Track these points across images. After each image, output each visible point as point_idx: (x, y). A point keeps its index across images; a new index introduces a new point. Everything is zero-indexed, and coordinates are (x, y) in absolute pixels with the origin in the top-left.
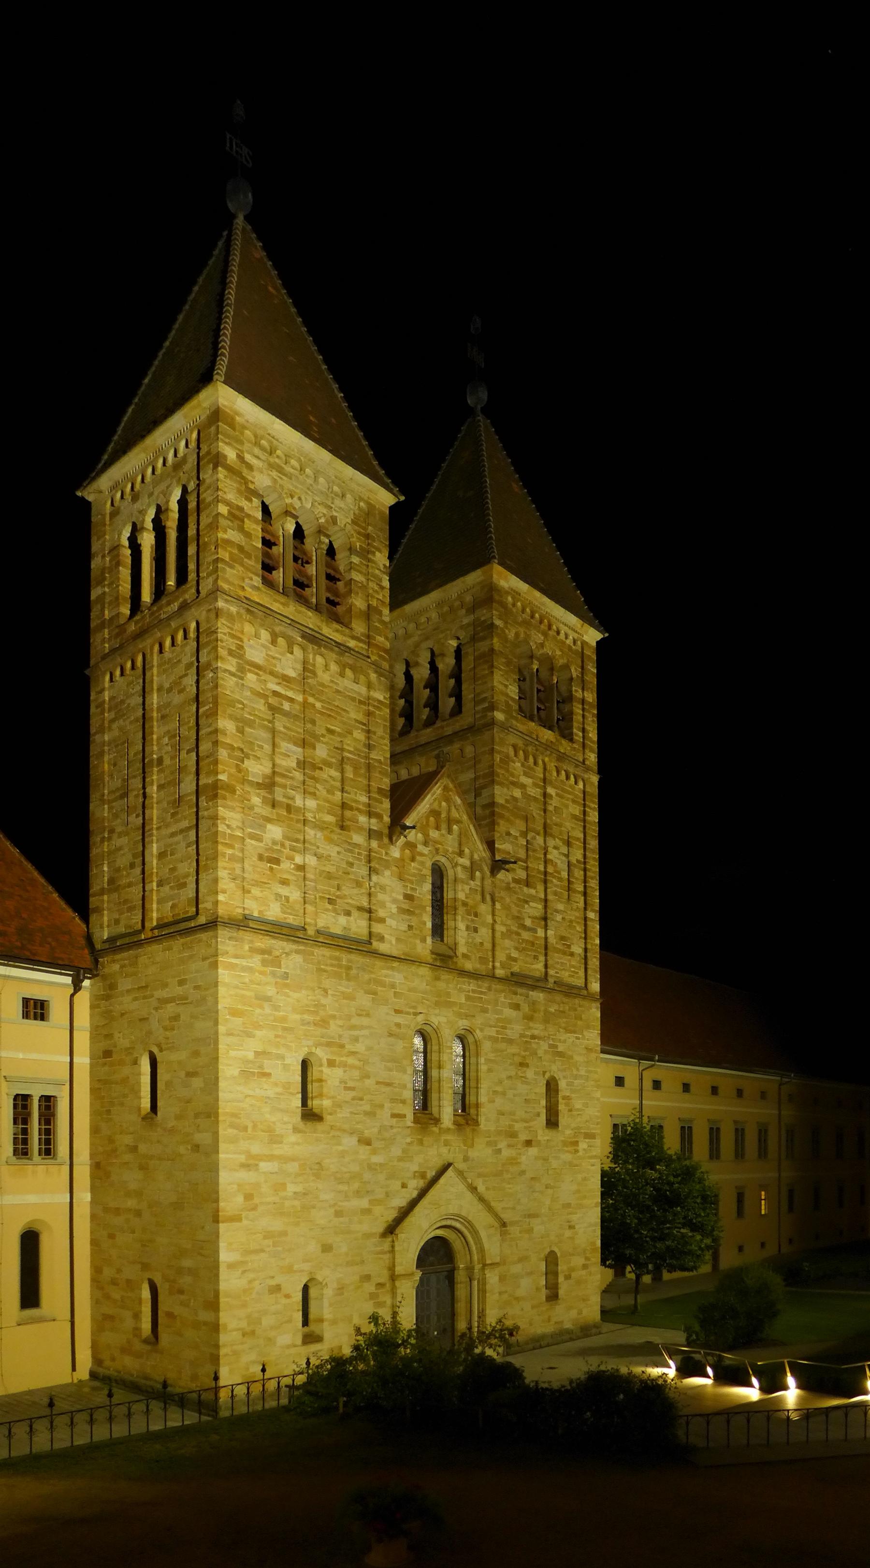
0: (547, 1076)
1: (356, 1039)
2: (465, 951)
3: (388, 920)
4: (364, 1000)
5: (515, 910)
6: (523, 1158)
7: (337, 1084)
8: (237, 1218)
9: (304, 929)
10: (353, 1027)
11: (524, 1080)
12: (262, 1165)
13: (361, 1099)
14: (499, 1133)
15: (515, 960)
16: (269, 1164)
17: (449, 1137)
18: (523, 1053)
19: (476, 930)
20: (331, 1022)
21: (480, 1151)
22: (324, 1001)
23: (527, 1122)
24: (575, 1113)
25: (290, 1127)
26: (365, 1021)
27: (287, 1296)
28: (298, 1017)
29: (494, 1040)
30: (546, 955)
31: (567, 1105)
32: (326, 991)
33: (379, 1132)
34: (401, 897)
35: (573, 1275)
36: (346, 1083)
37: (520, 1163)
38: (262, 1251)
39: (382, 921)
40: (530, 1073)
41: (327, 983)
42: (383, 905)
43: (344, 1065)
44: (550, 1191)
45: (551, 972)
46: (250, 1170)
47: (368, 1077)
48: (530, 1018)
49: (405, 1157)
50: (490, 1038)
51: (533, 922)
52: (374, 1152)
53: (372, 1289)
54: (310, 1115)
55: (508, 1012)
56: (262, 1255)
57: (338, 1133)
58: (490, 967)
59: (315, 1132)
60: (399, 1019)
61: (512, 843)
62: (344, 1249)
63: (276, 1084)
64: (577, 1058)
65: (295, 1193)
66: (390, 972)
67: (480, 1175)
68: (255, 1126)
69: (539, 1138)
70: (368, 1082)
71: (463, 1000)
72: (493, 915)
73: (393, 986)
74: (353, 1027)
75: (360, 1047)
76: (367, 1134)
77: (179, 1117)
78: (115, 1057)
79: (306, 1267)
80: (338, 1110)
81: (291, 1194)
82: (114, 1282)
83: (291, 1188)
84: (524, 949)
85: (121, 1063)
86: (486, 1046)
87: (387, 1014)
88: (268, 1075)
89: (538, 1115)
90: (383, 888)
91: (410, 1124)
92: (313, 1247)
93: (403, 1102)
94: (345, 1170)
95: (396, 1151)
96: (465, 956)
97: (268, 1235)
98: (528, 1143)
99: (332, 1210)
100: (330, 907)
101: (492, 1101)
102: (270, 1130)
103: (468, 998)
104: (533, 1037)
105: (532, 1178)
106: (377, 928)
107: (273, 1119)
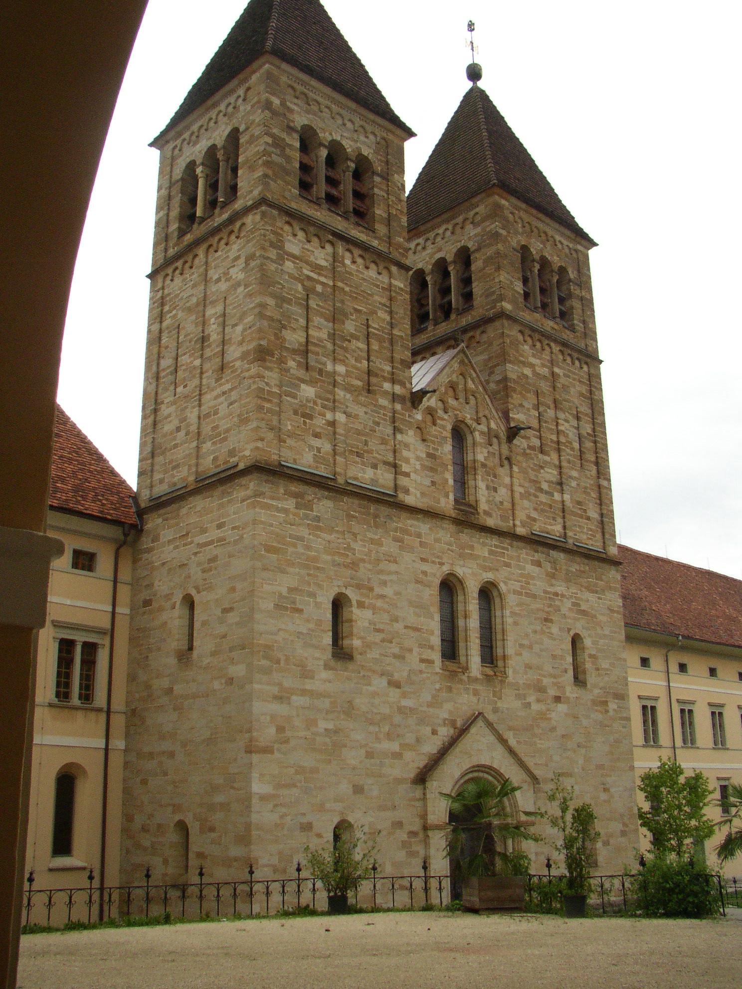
0: (572, 633)
1: (384, 583)
2: (486, 508)
3: (413, 476)
4: (390, 546)
5: (532, 475)
6: (553, 715)
7: (366, 624)
8: (267, 750)
9: (334, 480)
10: (381, 572)
11: (551, 636)
12: (294, 698)
13: (391, 642)
14: (528, 686)
15: (534, 520)
16: (302, 698)
17: (478, 687)
18: (547, 609)
19: (495, 490)
20: (361, 565)
21: (509, 702)
22: (353, 545)
23: (555, 677)
25: (322, 663)
26: (393, 567)
27: (319, 836)
28: (329, 558)
30: (564, 517)
31: (593, 663)
33: (409, 676)
34: (424, 456)
35: (612, 841)
36: (375, 625)
37: (550, 719)
38: (296, 786)
39: (407, 475)
40: (555, 630)
41: (356, 528)
42: (407, 461)
43: (373, 608)
44: (583, 751)
45: (570, 534)
46: (282, 703)
47: (396, 620)
48: (553, 576)
49: (435, 703)
50: (515, 592)
51: (549, 486)
52: (404, 695)
53: (405, 837)
56: (294, 790)
57: (369, 674)
58: (511, 524)
59: (345, 671)
60: (425, 567)
61: (525, 414)
62: (375, 793)
63: (308, 621)
65: (326, 730)
66: (416, 523)
68: (287, 659)
69: (568, 694)
70: (395, 625)
71: (486, 554)
72: (511, 477)
73: (419, 535)
74: (381, 572)
75: (388, 591)
76: (396, 676)
77: (214, 654)
78: (155, 605)
79: (339, 806)
80: (368, 651)
81: (322, 730)
82: (144, 829)
83: (323, 725)
84: (543, 511)
85: (160, 609)
86: (511, 600)
87: (414, 561)
88: (300, 611)
89: (566, 671)
90: (407, 446)
91: (438, 670)
92: (345, 788)
93: (432, 648)
94: (375, 711)
95: (427, 697)
96: (486, 513)
97: (300, 770)
98: (558, 699)
99: (363, 752)
100: (358, 459)
102: (302, 665)
103: (491, 552)
105: (563, 736)
106: (403, 481)
107: (306, 655)
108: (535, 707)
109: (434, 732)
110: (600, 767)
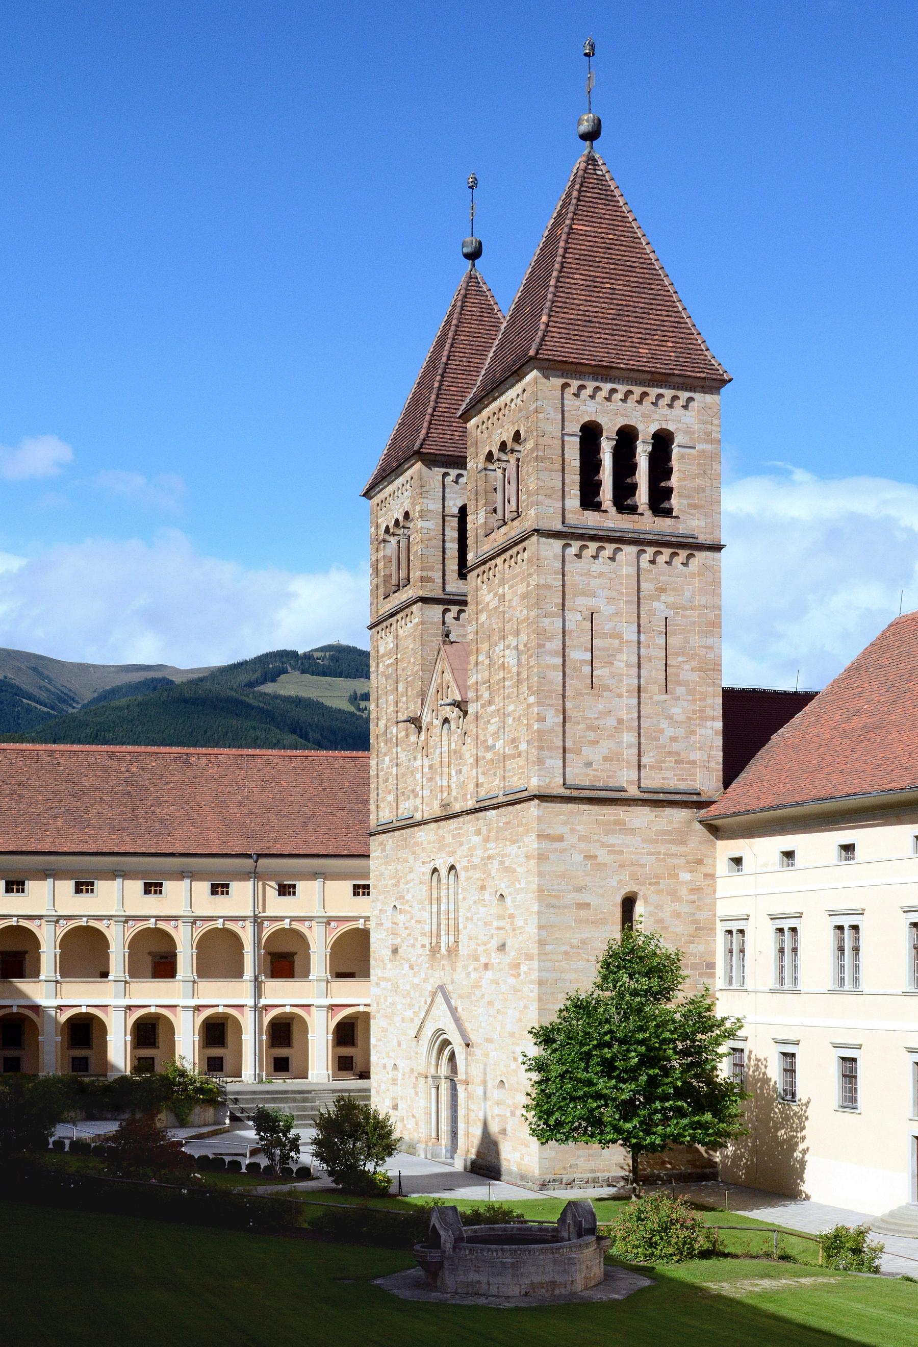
24: (517, 932)
29: (466, 869)
32: (398, 859)
40: (487, 896)
44: (500, 1017)
47: (412, 918)
48: (487, 840)
55: (475, 839)
64: (520, 870)
67: (460, 997)
69: (493, 961)
74: (407, 883)
84: (488, 770)
92: (395, 1043)
95: (423, 975)
101: (465, 928)
103: (454, 837)
104: (489, 858)
108: (474, 976)
110: (512, 1035)
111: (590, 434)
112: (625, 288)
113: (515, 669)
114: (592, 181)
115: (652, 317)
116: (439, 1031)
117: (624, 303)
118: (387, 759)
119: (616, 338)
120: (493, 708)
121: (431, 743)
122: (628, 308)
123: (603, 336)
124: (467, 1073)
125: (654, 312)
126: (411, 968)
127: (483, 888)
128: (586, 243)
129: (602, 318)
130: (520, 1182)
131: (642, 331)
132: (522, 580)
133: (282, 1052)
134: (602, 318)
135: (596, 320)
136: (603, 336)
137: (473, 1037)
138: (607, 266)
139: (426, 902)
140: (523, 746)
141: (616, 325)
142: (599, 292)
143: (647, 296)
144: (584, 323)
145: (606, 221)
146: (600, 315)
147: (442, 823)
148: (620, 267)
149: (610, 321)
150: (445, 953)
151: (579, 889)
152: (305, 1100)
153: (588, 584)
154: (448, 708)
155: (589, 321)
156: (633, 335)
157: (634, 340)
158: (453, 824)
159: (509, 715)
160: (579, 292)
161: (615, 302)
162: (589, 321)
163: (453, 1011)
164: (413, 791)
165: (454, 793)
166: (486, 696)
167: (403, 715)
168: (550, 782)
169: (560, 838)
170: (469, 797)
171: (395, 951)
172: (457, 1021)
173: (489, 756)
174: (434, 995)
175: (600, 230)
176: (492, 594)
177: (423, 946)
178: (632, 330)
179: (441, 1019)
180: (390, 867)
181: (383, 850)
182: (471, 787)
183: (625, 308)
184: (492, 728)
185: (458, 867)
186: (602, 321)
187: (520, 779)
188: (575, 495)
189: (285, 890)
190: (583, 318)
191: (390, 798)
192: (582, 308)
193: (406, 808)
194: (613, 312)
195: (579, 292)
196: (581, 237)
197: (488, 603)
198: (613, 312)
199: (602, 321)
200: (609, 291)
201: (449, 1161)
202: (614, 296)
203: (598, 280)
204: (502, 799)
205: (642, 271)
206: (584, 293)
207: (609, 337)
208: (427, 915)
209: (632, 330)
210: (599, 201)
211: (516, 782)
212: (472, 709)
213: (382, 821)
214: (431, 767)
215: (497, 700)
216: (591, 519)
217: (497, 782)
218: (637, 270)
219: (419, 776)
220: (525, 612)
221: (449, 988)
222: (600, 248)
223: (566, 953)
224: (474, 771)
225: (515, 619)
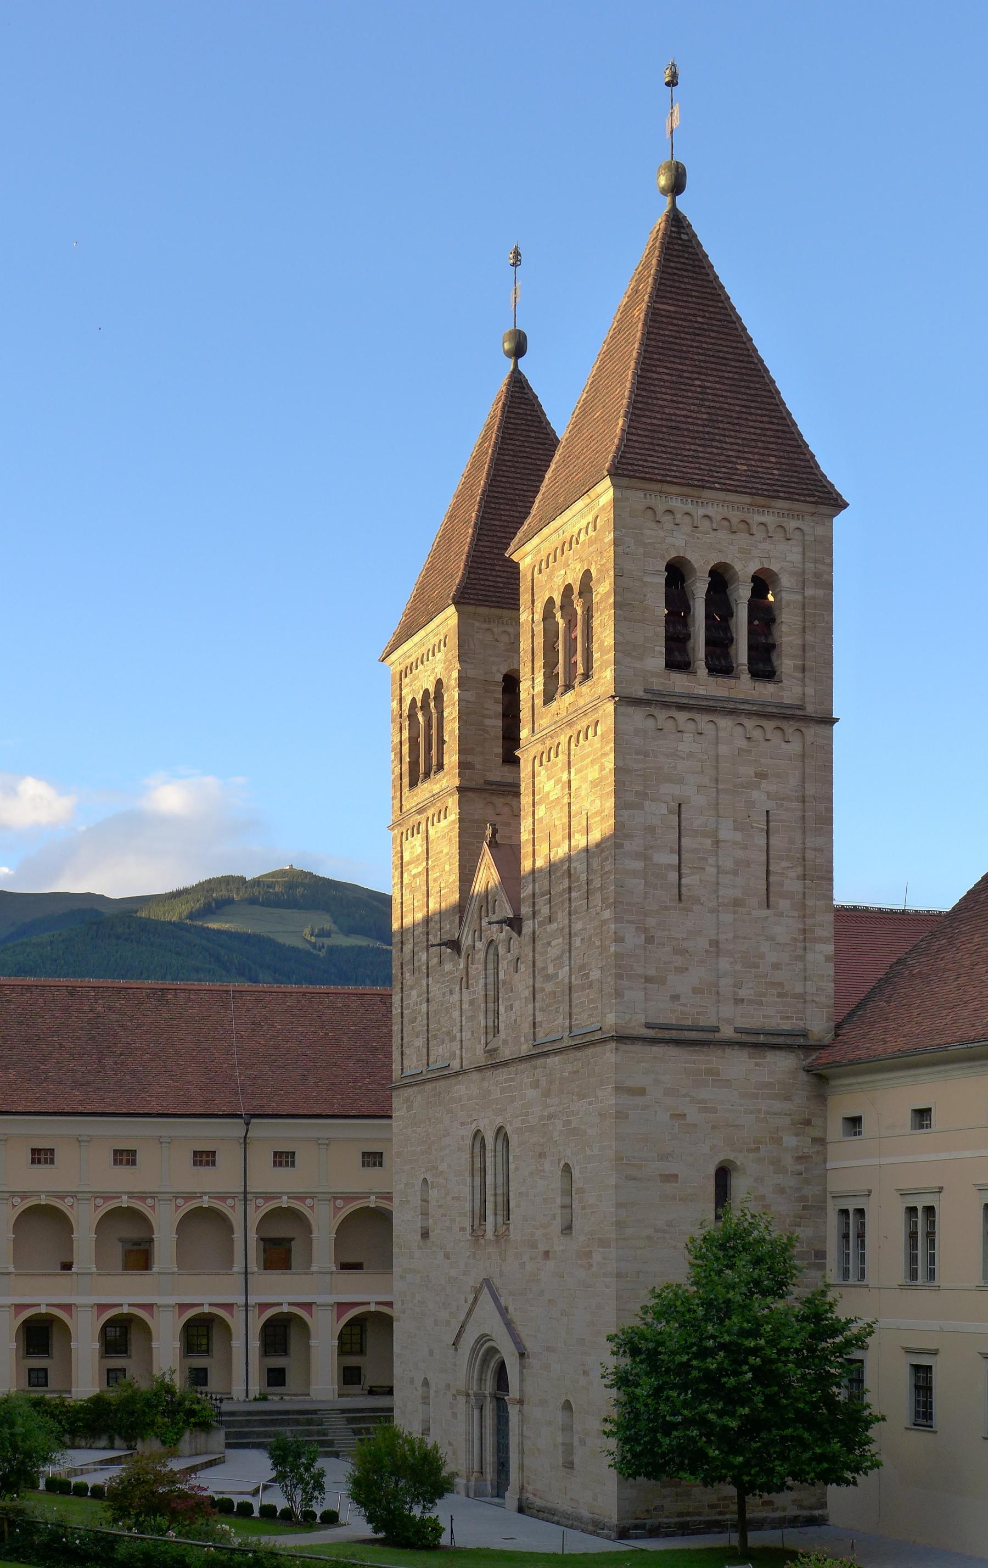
32: (429, 1119)
48: (547, 1094)
54: (425, 1234)
55: (531, 1093)
91: (470, 1238)
101: (518, 1206)
104: (550, 1117)
109: (466, 1302)
111: (677, 573)
112: (717, 386)
113: (583, 877)
114: (676, 247)
115: (751, 424)
116: (484, 1339)
117: (717, 405)
118: (414, 993)
119: (709, 450)
120: (554, 926)
121: (472, 972)
122: (723, 412)
123: (693, 447)
124: (521, 1391)
125: (754, 418)
126: (447, 1256)
127: (542, 1155)
128: (670, 327)
129: (692, 424)
130: (590, 1528)
131: (739, 441)
132: (593, 762)
133: (277, 1362)
134: (692, 424)
135: (685, 426)
136: (693, 447)
137: (529, 1345)
138: (696, 357)
139: (467, 1174)
140: (595, 974)
141: (708, 433)
142: (687, 391)
143: (744, 397)
144: (670, 431)
145: (694, 300)
146: (690, 420)
147: (488, 1073)
148: (712, 359)
149: (701, 429)
150: (492, 1238)
151: (663, 1157)
152: (309, 1422)
153: (675, 767)
154: (495, 927)
155: (676, 428)
156: (728, 446)
157: (731, 453)
158: (502, 1075)
159: (576, 935)
160: (663, 390)
161: (707, 403)
162: (676, 428)
163: (503, 1311)
164: (449, 1033)
165: (502, 1035)
166: (545, 910)
167: (435, 937)
168: (630, 1020)
169: (642, 1092)
170: (523, 1039)
171: (425, 1234)
172: (509, 1324)
173: (549, 987)
174: (477, 1292)
175: (686, 311)
176: (552, 781)
177: (463, 1229)
178: (728, 440)
179: (487, 1321)
180: (419, 1130)
181: (410, 1108)
182: (526, 1028)
183: (719, 412)
184: (553, 952)
185: (509, 1129)
186: (691, 427)
187: (590, 1016)
188: (660, 652)
189: (284, 1159)
190: (669, 424)
191: (420, 1042)
192: (667, 410)
193: (441, 1054)
194: (705, 416)
195: (663, 390)
196: (664, 320)
197: (548, 793)
198: (705, 416)
199: (691, 427)
200: (699, 389)
201: (497, 1500)
202: (706, 396)
203: (686, 375)
204: (567, 1042)
205: (738, 364)
206: (669, 392)
207: (700, 449)
208: (468, 1190)
209: (728, 440)
210: (685, 274)
211: (586, 1021)
212: (527, 927)
213: (408, 1072)
214: (472, 1003)
215: (560, 915)
216: (679, 682)
217: (560, 1020)
218: (733, 364)
219: (456, 1014)
220: (598, 802)
221: (497, 1282)
222: (688, 333)
223: (649, 1238)
224: (530, 1006)
225: (584, 813)
